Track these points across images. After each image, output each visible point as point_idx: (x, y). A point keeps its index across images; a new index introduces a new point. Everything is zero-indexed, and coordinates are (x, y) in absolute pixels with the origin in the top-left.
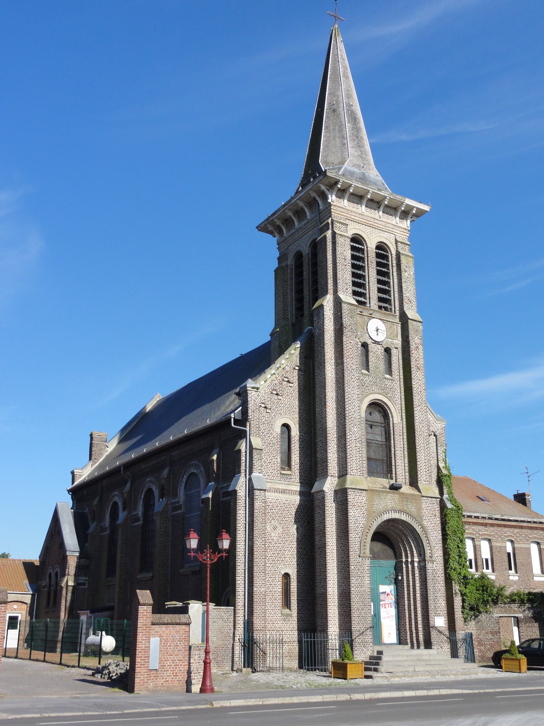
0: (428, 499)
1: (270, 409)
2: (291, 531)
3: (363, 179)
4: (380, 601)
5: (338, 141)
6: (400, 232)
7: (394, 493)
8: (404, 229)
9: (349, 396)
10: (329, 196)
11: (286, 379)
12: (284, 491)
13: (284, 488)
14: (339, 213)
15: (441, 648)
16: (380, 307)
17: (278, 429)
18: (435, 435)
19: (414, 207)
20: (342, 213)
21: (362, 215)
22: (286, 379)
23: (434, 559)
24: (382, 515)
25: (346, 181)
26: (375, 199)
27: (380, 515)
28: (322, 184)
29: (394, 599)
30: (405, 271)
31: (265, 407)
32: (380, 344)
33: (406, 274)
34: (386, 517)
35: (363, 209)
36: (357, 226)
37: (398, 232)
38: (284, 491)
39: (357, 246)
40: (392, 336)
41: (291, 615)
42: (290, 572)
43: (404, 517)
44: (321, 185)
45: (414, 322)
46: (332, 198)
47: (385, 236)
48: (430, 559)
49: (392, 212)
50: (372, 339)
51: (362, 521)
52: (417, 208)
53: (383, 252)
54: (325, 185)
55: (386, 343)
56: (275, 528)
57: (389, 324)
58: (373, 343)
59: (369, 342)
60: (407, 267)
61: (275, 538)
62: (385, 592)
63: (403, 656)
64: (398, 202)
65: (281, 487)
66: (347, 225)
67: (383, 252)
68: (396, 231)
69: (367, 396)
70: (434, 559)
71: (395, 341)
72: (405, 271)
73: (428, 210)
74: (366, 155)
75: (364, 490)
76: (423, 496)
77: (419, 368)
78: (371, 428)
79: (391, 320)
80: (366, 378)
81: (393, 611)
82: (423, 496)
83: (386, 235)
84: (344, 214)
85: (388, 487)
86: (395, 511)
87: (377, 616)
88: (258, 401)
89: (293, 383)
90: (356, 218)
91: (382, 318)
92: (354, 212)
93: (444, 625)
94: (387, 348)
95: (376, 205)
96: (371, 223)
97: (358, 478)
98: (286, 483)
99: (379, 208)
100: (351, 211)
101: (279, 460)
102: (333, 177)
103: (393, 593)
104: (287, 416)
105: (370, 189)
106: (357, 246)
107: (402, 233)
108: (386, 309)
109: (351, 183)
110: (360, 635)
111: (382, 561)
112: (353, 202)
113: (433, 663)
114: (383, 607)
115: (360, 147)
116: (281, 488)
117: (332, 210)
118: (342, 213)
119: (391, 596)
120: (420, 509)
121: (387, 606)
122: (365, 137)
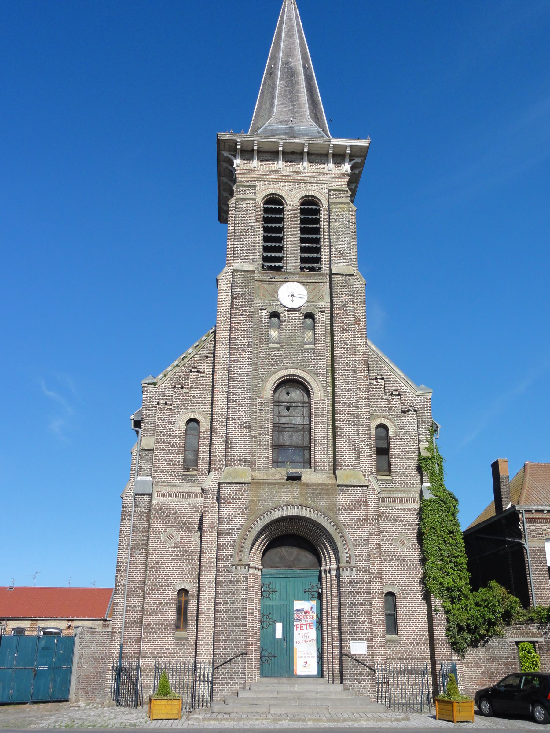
0: (349, 488)
1: (171, 404)
2: (193, 539)
3: (291, 133)
4: (294, 620)
5: (268, 103)
6: (334, 180)
7: (291, 485)
8: (341, 174)
9: (236, 375)
10: (234, 161)
11: (196, 370)
12: (186, 495)
13: (186, 491)
14: (247, 176)
15: (359, 683)
16: (302, 269)
17: (181, 425)
18: (415, 411)
19: (346, 146)
20: (251, 176)
21: (278, 172)
22: (196, 370)
23: (353, 564)
24: (271, 513)
25: (246, 139)
26: (296, 151)
27: (270, 511)
28: (225, 150)
29: (315, 617)
30: (336, 221)
31: (166, 403)
32: (297, 311)
33: (338, 224)
34: (278, 514)
35: (280, 164)
36: (272, 185)
37: (332, 180)
38: (186, 495)
39: (277, 207)
40: (315, 299)
41: (187, 639)
42: (188, 588)
43: (306, 513)
44: (222, 152)
45: (341, 277)
46: (238, 162)
48: (348, 565)
49: (323, 159)
50: (285, 306)
51: (239, 521)
52: (351, 146)
53: (314, 207)
54: (229, 151)
55: (307, 308)
56: (170, 537)
57: (311, 286)
58: (288, 311)
59: (281, 310)
60: (338, 216)
61: (170, 549)
62: (303, 610)
63: (271, 692)
64: (324, 146)
65: (181, 490)
66: (255, 187)
67: (314, 207)
68: (329, 179)
69: (274, 373)
70: (353, 564)
71: (320, 304)
72: (336, 221)
73: (368, 145)
74: (300, 107)
75: (245, 484)
76: (339, 486)
77: (346, 330)
78: (288, 410)
79: (314, 281)
80: (276, 352)
81: (313, 634)
82: (339, 486)
84: (253, 176)
85: (286, 478)
86: (293, 506)
87: (288, 640)
88: (156, 398)
89: (204, 373)
90: (270, 177)
91: (300, 281)
92: (268, 171)
93: (366, 653)
95: (299, 157)
96: (291, 178)
97: (240, 469)
98: (188, 485)
99: (278, 158)
100: (264, 171)
101: (181, 460)
102: (228, 138)
103: (314, 610)
104: (195, 410)
105: (280, 141)
106: (277, 207)
107: (337, 180)
108: (312, 269)
109: (252, 139)
110: (226, 663)
111: (298, 571)
112: (267, 161)
113: (313, 702)
114: (299, 629)
115: (292, 101)
116: (182, 491)
117: (237, 176)
118: (251, 176)
119: (311, 614)
120: (333, 502)
121: (304, 627)
122: (302, 90)
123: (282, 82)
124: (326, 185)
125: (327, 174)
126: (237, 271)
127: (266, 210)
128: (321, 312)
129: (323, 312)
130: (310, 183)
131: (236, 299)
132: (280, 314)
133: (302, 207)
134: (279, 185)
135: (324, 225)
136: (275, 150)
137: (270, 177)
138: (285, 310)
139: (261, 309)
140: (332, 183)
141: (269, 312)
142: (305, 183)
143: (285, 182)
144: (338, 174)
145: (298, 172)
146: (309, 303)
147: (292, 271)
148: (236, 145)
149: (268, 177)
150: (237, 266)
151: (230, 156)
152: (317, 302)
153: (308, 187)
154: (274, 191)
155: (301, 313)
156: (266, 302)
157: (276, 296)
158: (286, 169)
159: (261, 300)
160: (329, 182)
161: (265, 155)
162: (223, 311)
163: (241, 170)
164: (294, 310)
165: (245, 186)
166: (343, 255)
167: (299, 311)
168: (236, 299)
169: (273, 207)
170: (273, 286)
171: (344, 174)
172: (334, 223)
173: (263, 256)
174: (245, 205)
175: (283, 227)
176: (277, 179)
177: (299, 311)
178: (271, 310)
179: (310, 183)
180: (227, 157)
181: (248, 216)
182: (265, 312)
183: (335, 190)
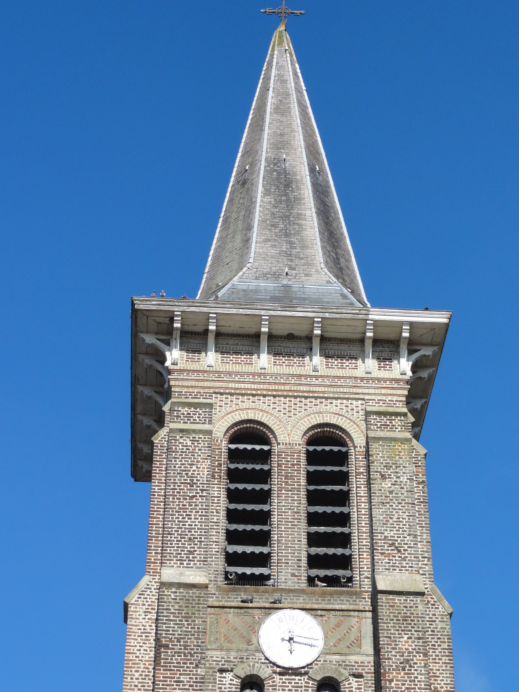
3: (286, 298)
5: (239, 238)
6: (377, 391)
8: (392, 380)
10: (168, 354)
14: (193, 383)
16: (311, 581)
19: (402, 323)
20: (201, 384)
21: (260, 375)
25: (192, 309)
26: (296, 333)
28: (147, 332)
32: (301, 674)
33: (387, 484)
35: (264, 360)
36: (247, 402)
39: (258, 447)
40: (342, 647)
44: (143, 335)
45: (397, 598)
46: (174, 356)
47: (334, 409)
49: (354, 350)
50: (274, 664)
53: (336, 449)
54: (157, 333)
55: (323, 668)
57: (333, 619)
58: (280, 674)
59: (265, 672)
64: (355, 323)
67: (336, 449)
68: (367, 391)
71: (353, 658)
73: (446, 321)
74: (304, 247)
79: (337, 607)
83: (335, 406)
90: (243, 386)
91: (308, 606)
92: (237, 373)
94: (325, 678)
95: (304, 345)
96: (287, 388)
99: (258, 347)
100: (230, 374)
102: (155, 308)
105: (263, 312)
106: (258, 447)
107: (383, 391)
108: (332, 581)
109: (205, 310)
112: (237, 353)
115: (287, 235)
117: (172, 383)
118: (201, 384)
122: (308, 213)
123: (267, 199)
124: (360, 402)
125: (362, 379)
126: (170, 585)
127: (233, 456)
128: (355, 676)
129: (359, 676)
130: (327, 398)
131: (167, 647)
132: (262, 681)
133: (311, 448)
134: (260, 403)
135: (357, 486)
136: (253, 331)
137: (243, 386)
138: (275, 672)
139: (221, 671)
140: (373, 397)
141: (238, 677)
142: (316, 398)
143: (275, 396)
144: (385, 380)
145: (300, 376)
146: (328, 657)
147: (291, 584)
148: (172, 320)
149: (237, 386)
150: (169, 574)
151: (159, 343)
152: (346, 655)
153: (322, 407)
154: (251, 415)
155: (310, 678)
156: (233, 654)
157: (254, 641)
158: (276, 369)
159: (222, 650)
160: (367, 397)
161: (231, 342)
162: (137, 675)
163: (181, 371)
164: (295, 672)
165: (190, 405)
166: (399, 551)
167: (306, 673)
168: (167, 647)
169: (249, 447)
170: (248, 619)
171: (397, 381)
172: (379, 481)
173: (227, 553)
174: (189, 443)
175: (270, 490)
176: (257, 390)
177: (306, 673)
178: (243, 671)
179: (327, 398)
180: (152, 346)
181: (194, 468)
182: (229, 676)
183: (379, 414)
